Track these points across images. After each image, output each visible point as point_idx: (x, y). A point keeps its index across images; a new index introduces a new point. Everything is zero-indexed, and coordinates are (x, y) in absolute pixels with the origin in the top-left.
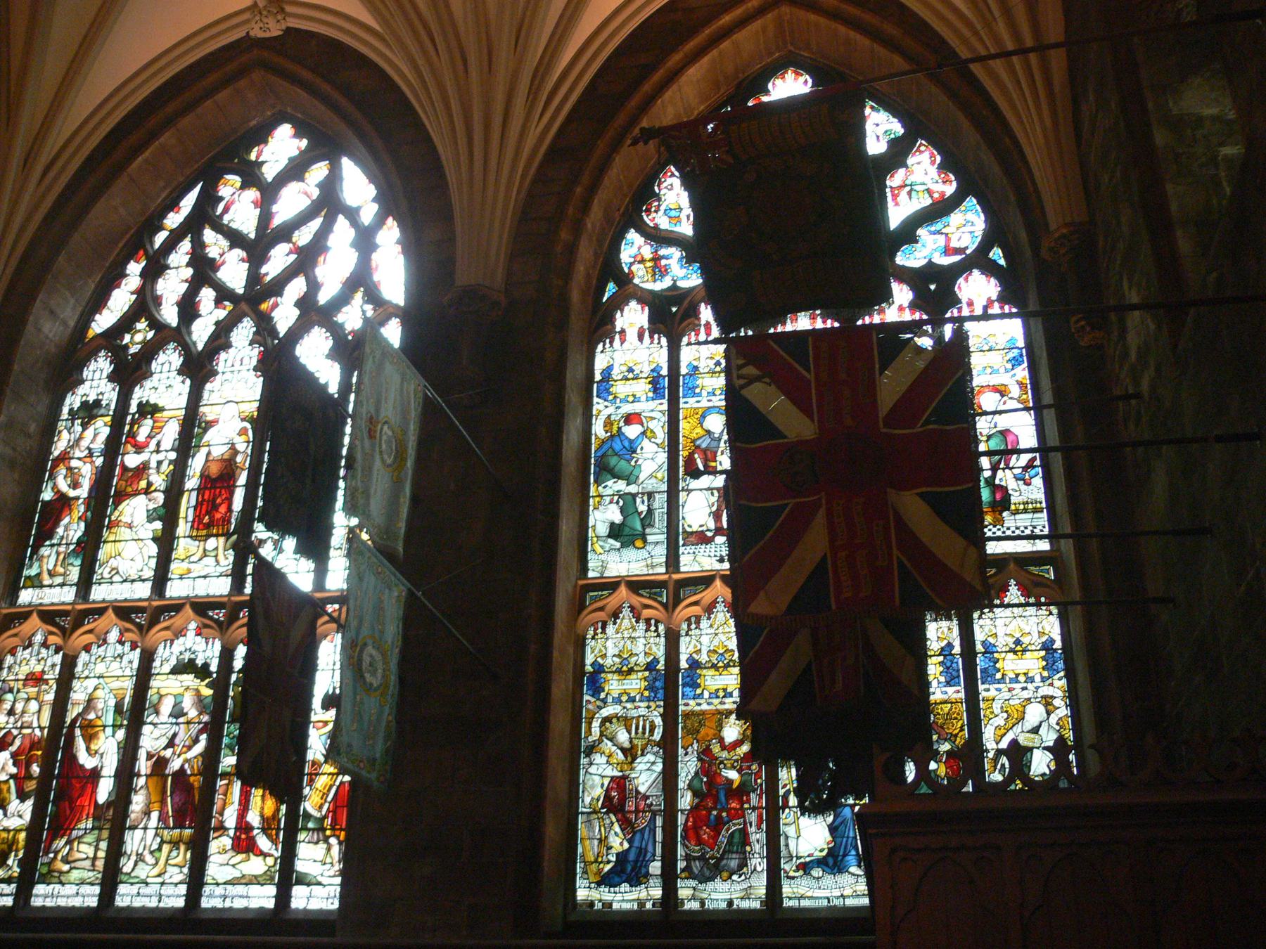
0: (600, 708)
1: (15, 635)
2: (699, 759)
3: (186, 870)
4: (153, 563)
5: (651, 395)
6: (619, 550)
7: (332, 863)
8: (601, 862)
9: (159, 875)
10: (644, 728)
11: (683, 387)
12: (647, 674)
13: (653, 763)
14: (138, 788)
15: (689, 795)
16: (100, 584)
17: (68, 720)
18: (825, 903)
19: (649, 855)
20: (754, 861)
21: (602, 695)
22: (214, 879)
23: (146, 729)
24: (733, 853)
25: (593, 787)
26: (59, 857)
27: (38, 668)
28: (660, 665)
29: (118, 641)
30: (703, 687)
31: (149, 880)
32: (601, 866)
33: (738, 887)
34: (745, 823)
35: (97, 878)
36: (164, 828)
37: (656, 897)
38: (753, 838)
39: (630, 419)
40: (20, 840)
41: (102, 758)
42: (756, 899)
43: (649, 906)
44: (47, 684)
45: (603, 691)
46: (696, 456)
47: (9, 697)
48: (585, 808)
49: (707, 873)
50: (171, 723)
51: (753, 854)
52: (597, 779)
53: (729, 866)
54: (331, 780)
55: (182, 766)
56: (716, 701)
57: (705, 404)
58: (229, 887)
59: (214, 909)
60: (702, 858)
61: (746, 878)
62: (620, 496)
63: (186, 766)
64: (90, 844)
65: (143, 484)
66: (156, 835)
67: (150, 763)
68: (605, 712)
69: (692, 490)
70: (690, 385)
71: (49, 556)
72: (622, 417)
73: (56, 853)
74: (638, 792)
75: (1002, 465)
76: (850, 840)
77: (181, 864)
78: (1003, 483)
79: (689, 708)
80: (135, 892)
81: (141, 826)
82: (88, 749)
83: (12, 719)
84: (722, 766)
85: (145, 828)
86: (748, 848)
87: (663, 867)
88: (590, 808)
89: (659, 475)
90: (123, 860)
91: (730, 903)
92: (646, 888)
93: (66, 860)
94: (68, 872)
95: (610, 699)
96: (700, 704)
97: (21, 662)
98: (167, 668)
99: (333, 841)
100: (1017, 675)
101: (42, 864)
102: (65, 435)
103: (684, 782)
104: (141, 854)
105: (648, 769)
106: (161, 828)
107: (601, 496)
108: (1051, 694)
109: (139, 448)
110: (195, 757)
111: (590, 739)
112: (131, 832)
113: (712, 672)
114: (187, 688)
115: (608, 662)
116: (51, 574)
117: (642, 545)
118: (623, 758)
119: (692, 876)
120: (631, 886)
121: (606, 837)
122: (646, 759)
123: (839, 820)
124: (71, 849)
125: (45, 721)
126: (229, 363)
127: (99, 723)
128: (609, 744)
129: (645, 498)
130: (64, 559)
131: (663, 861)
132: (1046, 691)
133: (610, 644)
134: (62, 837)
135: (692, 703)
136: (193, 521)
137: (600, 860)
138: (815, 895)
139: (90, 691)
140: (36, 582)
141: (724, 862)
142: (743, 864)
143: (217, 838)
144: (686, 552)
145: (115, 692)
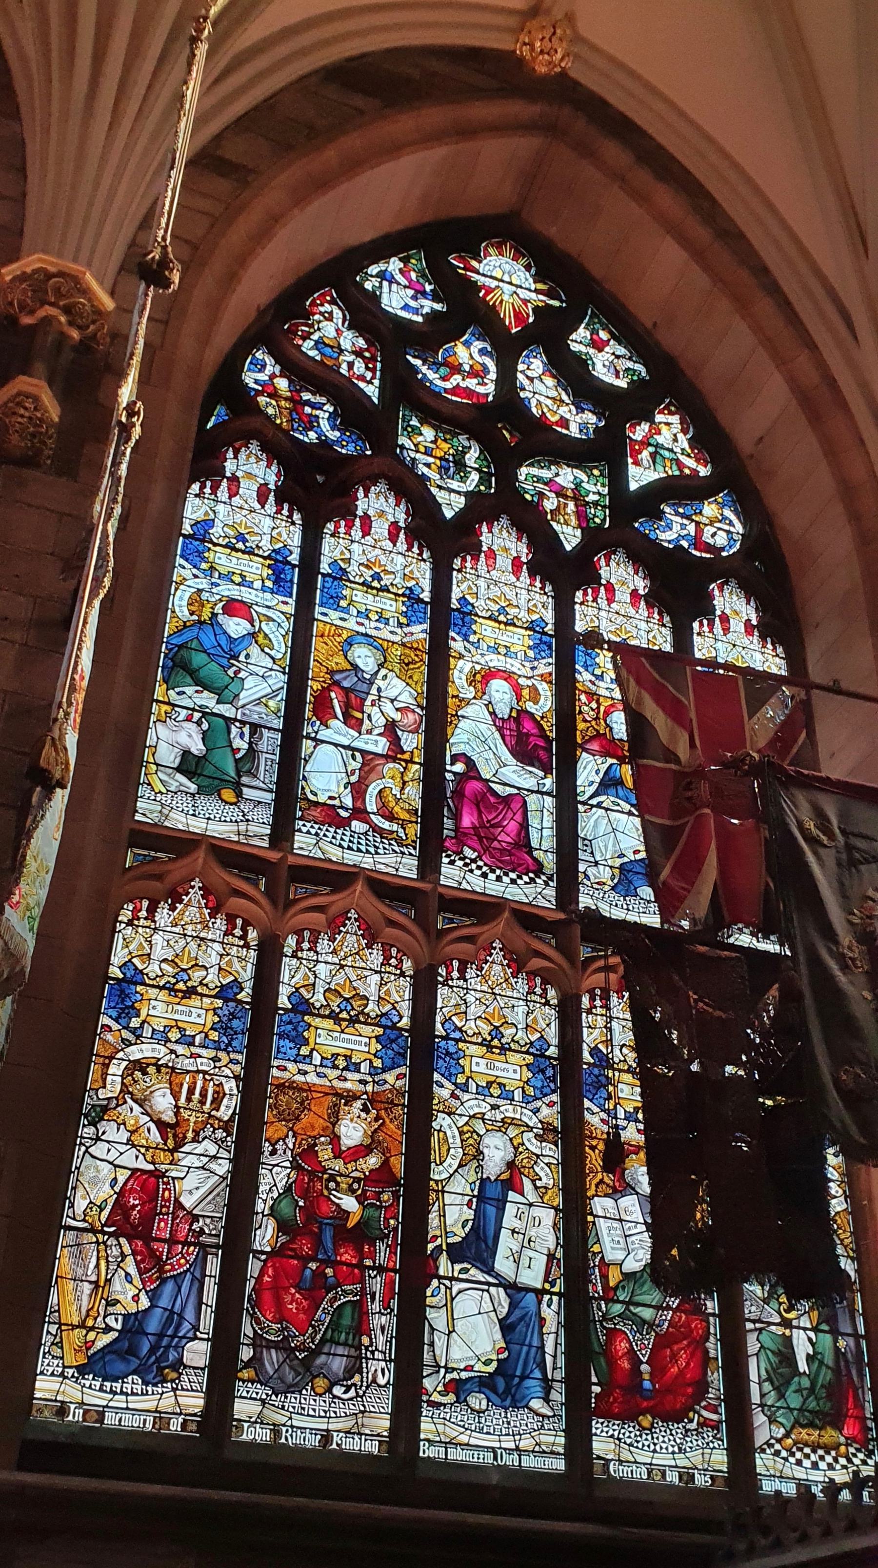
0: (128, 1043)
2: (295, 1166)
5: (269, 584)
6: (193, 795)
8: (92, 1328)
10: (204, 1095)
11: (322, 591)
12: (219, 1003)
15: (270, 1226)
18: (489, 1459)
19: (186, 1326)
20: (374, 1366)
21: (135, 1023)
24: (338, 1344)
25: (94, 1182)
28: (243, 993)
30: (312, 1045)
32: (92, 1336)
37: (191, 1411)
38: (378, 1321)
39: (233, 607)
43: (175, 1425)
45: (138, 1016)
46: (333, 695)
48: (74, 1219)
49: (290, 1377)
51: (373, 1352)
53: (330, 1369)
56: (333, 1074)
61: (357, 1395)
62: (205, 714)
68: (135, 1053)
69: (323, 742)
70: (332, 592)
72: (221, 600)
74: (179, 1205)
76: (533, 1350)
79: (286, 1075)
84: (332, 1185)
86: (365, 1340)
88: (84, 1220)
91: (326, 1437)
92: (174, 1390)
95: (147, 1032)
96: (305, 1073)
103: (265, 1201)
105: (203, 1168)
111: (102, 1094)
113: (328, 1024)
115: (153, 969)
117: (234, 800)
118: (159, 1140)
119: (260, 1379)
120: (146, 1383)
121: (108, 1281)
123: (518, 1313)
128: (137, 1108)
129: (246, 730)
133: (157, 938)
135: (291, 1066)
137: (90, 1323)
138: (473, 1441)
141: (322, 1359)
142: (355, 1368)
144: (304, 829)
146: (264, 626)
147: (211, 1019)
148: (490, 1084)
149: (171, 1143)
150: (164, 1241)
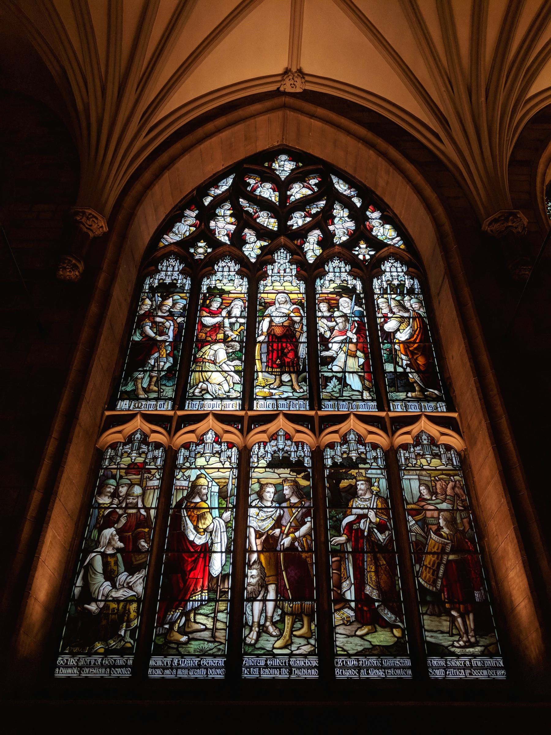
1: (119, 432)
3: (312, 642)
4: (239, 388)
7: (459, 634)
9: (285, 647)
14: (251, 562)
16: (192, 400)
17: (174, 503)
22: (344, 650)
23: (252, 511)
26: (176, 628)
27: (140, 460)
29: (214, 442)
31: (276, 651)
35: (219, 649)
36: (283, 601)
40: (132, 611)
41: (211, 535)
44: (150, 473)
47: (112, 481)
50: (275, 507)
54: (437, 558)
55: (292, 544)
58: (362, 659)
59: (349, 680)
63: (296, 544)
64: (207, 615)
65: (221, 336)
66: (276, 607)
67: (259, 541)
71: (143, 378)
73: (172, 624)
77: (306, 635)
80: (263, 663)
81: (259, 598)
82: (196, 528)
83: (116, 501)
85: (264, 600)
90: (246, 632)
93: (183, 631)
94: (186, 643)
97: (122, 454)
98: (263, 463)
99: (454, 613)
101: (156, 635)
102: (148, 301)
104: (264, 625)
106: (280, 600)
109: (213, 314)
110: (304, 536)
112: (249, 604)
114: (285, 480)
116: (147, 391)
124: (188, 620)
125: (152, 500)
126: (276, 271)
127: (205, 505)
130: (157, 381)
134: (177, 608)
136: (267, 362)
139: (193, 478)
140: (133, 396)
143: (339, 610)
145: (217, 481)
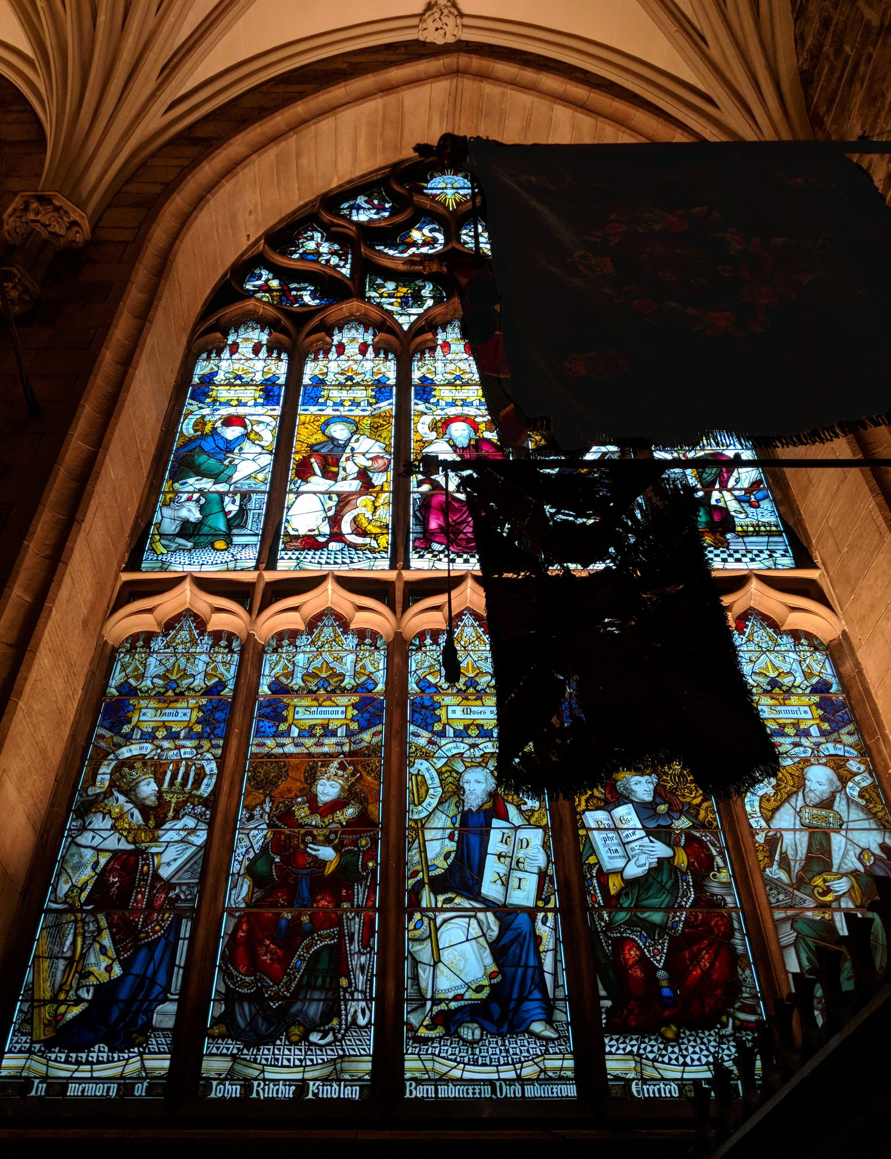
5: (261, 401)
8: (63, 1002)
11: (304, 396)
13: (193, 831)
18: (487, 1092)
19: (157, 990)
20: (353, 1007)
21: (126, 729)
24: (314, 988)
25: (78, 867)
28: (227, 690)
30: (290, 721)
32: (63, 1009)
33: (319, 1057)
34: (341, 936)
37: (157, 1073)
39: (229, 421)
42: (351, 1082)
43: (140, 1090)
45: (129, 721)
46: (313, 460)
48: (56, 902)
49: (263, 1028)
51: (352, 994)
52: (88, 854)
53: (306, 1015)
56: (309, 742)
57: (329, 411)
60: (256, 998)
61: (336, 1039)
68: (125, 753)
69: (302, 493)
70: (313, 395)
72: (220, 419)
74: (157, 877)
75: (717, 486)
76: (530, 971)
78: (722, 504)
79: (265, 750)
84: (309, 839)
86: (344, 982)
87: (179, 1014)
88: (65, 902)
89: (261, 476)
92: (141, 1054)
95: (137, 735)
96: (283, 745)
100: (782, 726)
103: (241, 863)
105: (182, 841)
107: (177, 492)
108: (841, 753)
111: (91, 791)
113: (307, 702)
117: (225, 547)
118: (141, 822)
119: (233, 1033)
120: (112, 1050)
121: (83, 956)
122: (180, 825)
123: (510, 935)
128: (122, 799)
129: (238, 498)
131: (181, 1003)
132: (830, 748)
133: (152, 661)
135: (270, 742)
137: (62, 996)
138: (467, 1075)
141: (297, 1006)
142: (333, 1010)
144: (286, 557)
146: (255, 428)
147: (196, 715)
148: (467, 727)
149: (152, 823)
150: (141, 911)
